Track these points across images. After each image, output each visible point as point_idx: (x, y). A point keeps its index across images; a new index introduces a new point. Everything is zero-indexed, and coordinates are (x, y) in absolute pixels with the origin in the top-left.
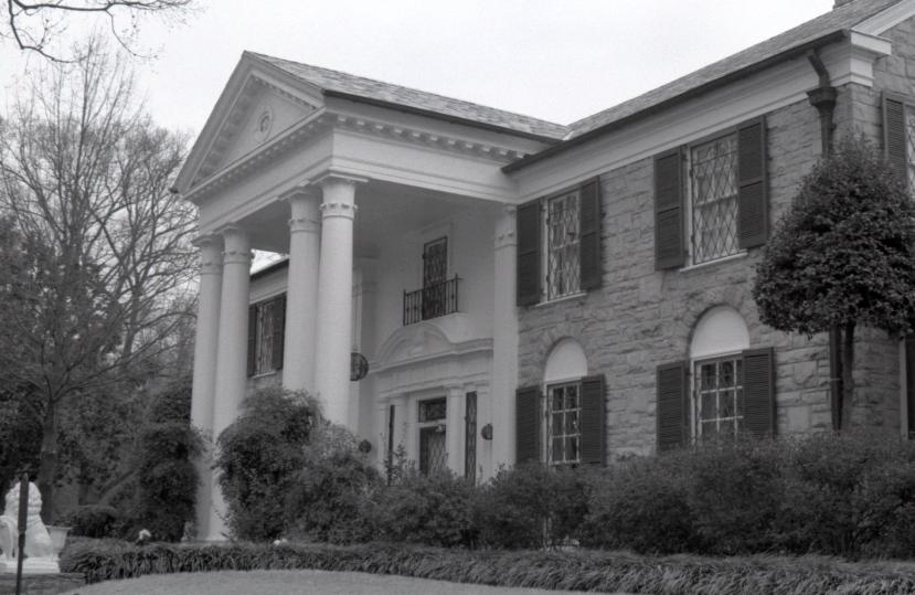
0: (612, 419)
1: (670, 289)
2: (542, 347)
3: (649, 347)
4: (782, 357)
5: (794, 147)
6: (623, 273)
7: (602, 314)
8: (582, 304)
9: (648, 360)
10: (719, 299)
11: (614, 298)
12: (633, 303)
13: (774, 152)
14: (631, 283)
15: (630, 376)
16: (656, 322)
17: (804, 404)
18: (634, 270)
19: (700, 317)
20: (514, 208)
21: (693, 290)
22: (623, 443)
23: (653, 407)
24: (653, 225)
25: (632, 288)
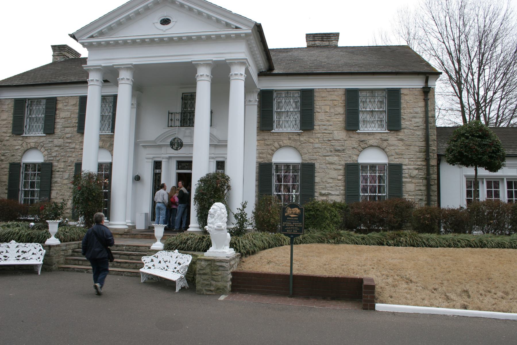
0: (317, 180)
1: (350, 137)
2: (273, 148)
3: (338, 156)
4: (404, 167)
5: (411, 102)
6: (325, 127)
7: (312, 140)
8: (299, 135)
9: (338, 162)
10: (375, 144)
11: (319, 135)
12: (330, 139)
13: (402, 101)
14: (329, 132)
15: (328, 165)
16: (343, 148)
17: (413, 183)
18: (330, 127)
19: (364, 149)
20: (259, 90)
21: (362, 139)
22: (323, 189)
23: (340, 177)
24: (342, 112)
25: (331, 133)
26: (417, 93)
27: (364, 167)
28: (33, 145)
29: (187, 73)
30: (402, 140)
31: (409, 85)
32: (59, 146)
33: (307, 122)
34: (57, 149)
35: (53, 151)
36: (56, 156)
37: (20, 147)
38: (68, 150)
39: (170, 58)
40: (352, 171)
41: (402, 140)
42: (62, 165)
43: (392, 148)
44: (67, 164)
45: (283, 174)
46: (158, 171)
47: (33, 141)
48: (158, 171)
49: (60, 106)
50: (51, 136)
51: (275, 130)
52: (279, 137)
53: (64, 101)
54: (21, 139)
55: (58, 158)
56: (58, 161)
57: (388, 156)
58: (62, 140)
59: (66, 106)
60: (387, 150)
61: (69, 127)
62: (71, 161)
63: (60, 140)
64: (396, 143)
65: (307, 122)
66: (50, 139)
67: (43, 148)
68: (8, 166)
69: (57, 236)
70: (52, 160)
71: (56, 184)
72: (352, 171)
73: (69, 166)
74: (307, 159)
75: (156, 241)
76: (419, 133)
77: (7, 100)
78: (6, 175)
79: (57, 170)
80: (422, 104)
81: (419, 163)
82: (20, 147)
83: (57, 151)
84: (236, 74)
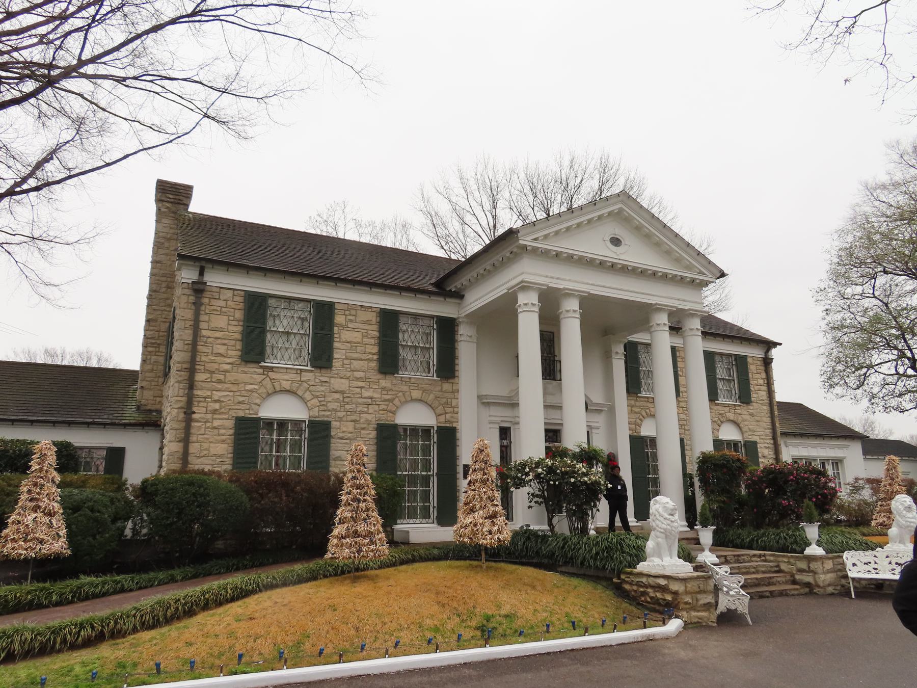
10: (732, 418)
26: (759, 363)
27: (269, 423)
28: (286, 385)
29: (641, 314)
30: (752, 415)
31: (753, 353)
32: (342, 392)
33: (322, 355)
34: (337, 396)
35: (330, 399)
36: (335, 410)
37: (256, 387)
38: (360, 400)
39: (598, 288)
40: (388, 436)
41: (752, 415)
42: (350, 427)
43: (746, 423)
44: (358, 426)
45: (275, 437)
46: (505, 443)
47: (286, 377)
48: (505, 443)
49: (339, 319)
50: (323, 371)
51: (643, 394)
52: (645, 404)
53: (347, 313)
54: (261, 371)
55: (340, 414)
56: (340, 420)
57: (742, 434)
58: (347, 382)
59: (351, 321)
60: (741, 425)
61: (361, 360)
62: (367, 420)
63: (343, 381)
64: (748, 417)
65: (322, 355)
66: (322, 376)
67: (308, 393)
68: (231, 423)
69: (819, 544)
70: (327, 416)
71: (338, 462)
72: (248, 430)
73: (363, 429)
74: (318, 414)
75: (703, 550)
76: (765, 408)
77: (226, 291)
78: (223, 441)
79: (341, 435)
80: (764, 375)
81: (768, 441)
82: (256, 387)
83: (337, 400)
84: (568, 311)
